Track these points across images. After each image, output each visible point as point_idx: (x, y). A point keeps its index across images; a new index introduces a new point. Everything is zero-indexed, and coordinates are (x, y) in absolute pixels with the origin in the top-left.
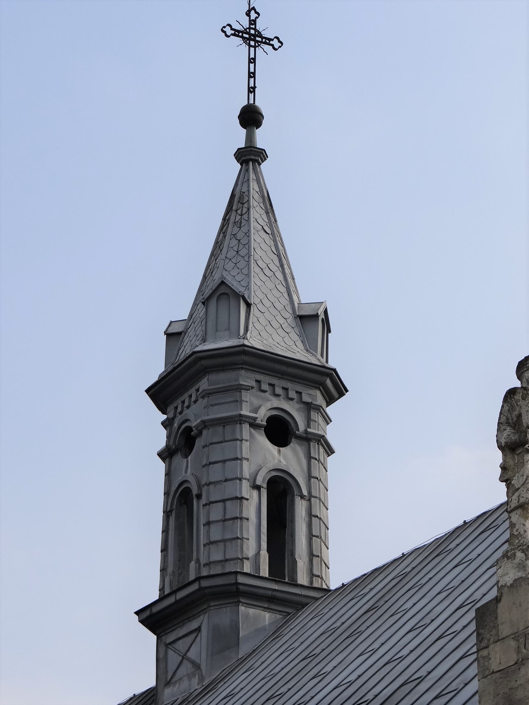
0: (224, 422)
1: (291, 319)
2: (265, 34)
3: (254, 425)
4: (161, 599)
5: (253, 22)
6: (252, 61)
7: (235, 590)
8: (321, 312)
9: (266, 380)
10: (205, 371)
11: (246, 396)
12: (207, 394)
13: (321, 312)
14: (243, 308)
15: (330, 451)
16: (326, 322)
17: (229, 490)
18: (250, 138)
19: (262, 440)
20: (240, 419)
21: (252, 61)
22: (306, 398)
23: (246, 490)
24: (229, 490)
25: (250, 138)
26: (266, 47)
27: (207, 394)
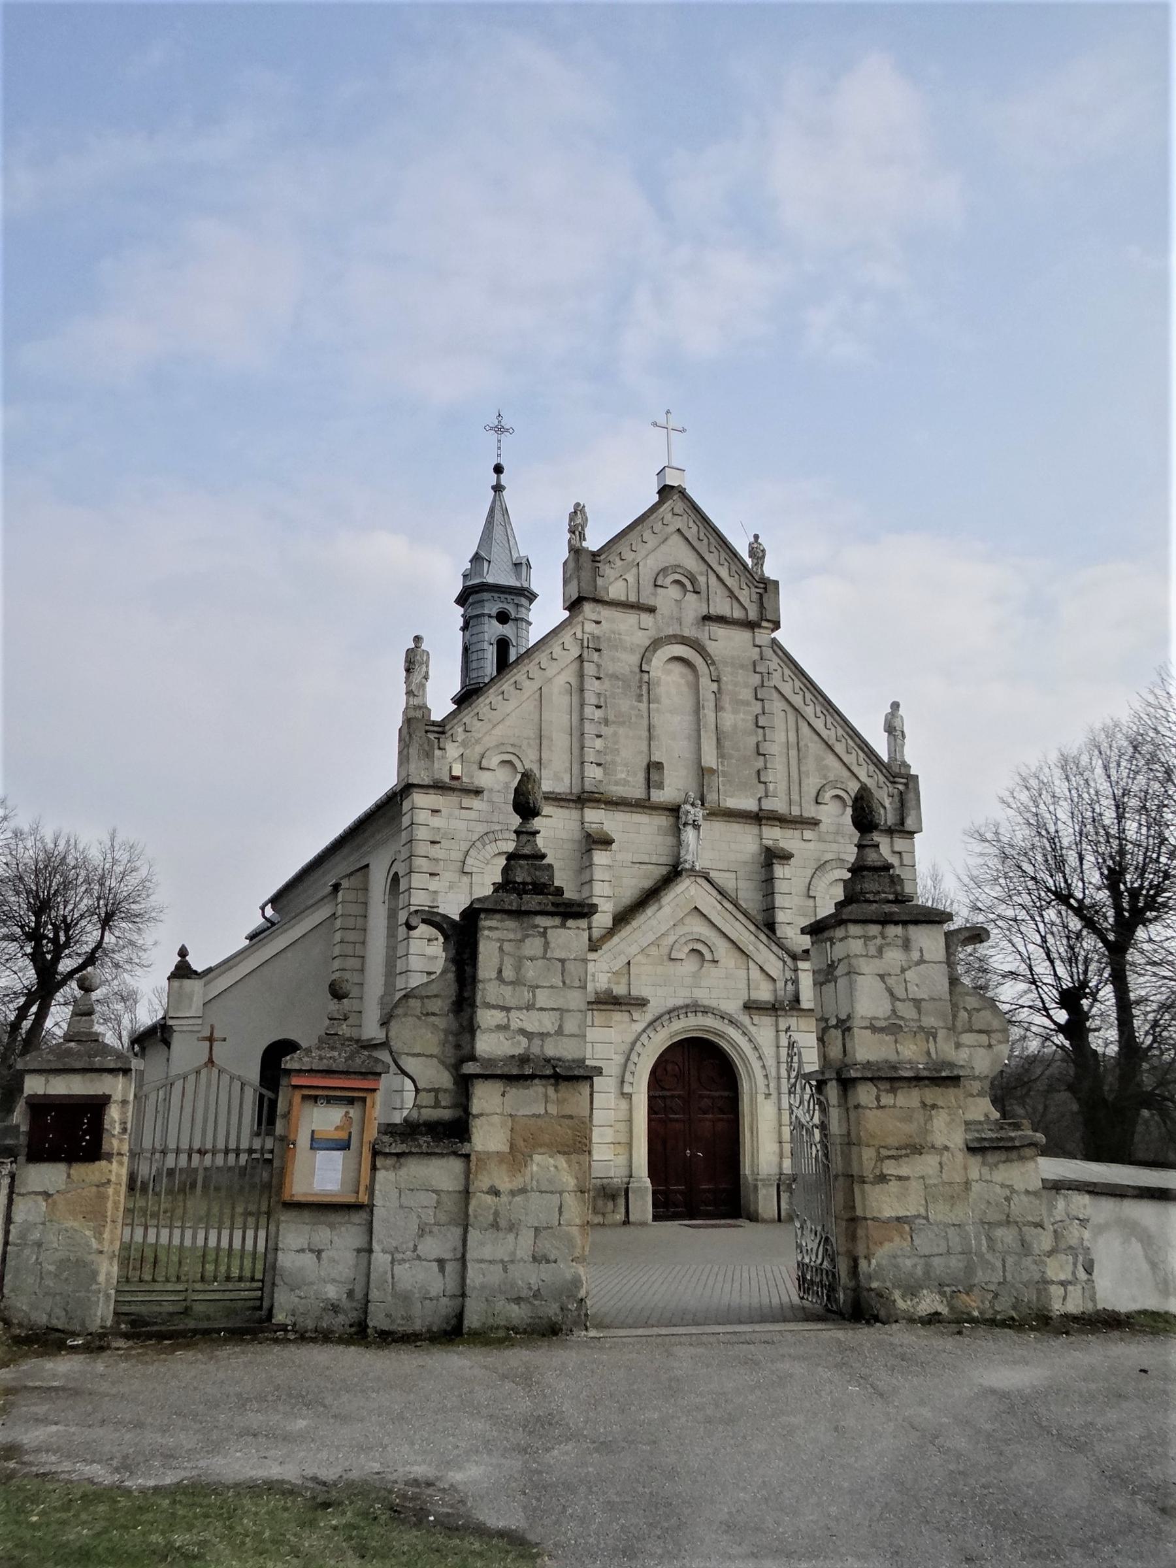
0: (477, 616)
1: (511, 566)
2: (506, 427)
3: (490, 616)
4: (462, 689)
5: (500, 422)
6: (499, 441)
7: (420, 716)
8: (524, 561)
9: (496, 595)
10: (486, 591)
11: (486, 604)
12: (472, 604)
13: (524, 561)
14: (486, 564)
15: (530, 624)
16: (529, 566)
17: (479, 646)
18: (498, 479)
19: (495, 622)
20: (483, 615)
21: (499, 441)
22: (516, 601)
23: (486, 646)
24: (479, 646)
25: (498, 479)
26: (491, 425)
27: (472, 604)
